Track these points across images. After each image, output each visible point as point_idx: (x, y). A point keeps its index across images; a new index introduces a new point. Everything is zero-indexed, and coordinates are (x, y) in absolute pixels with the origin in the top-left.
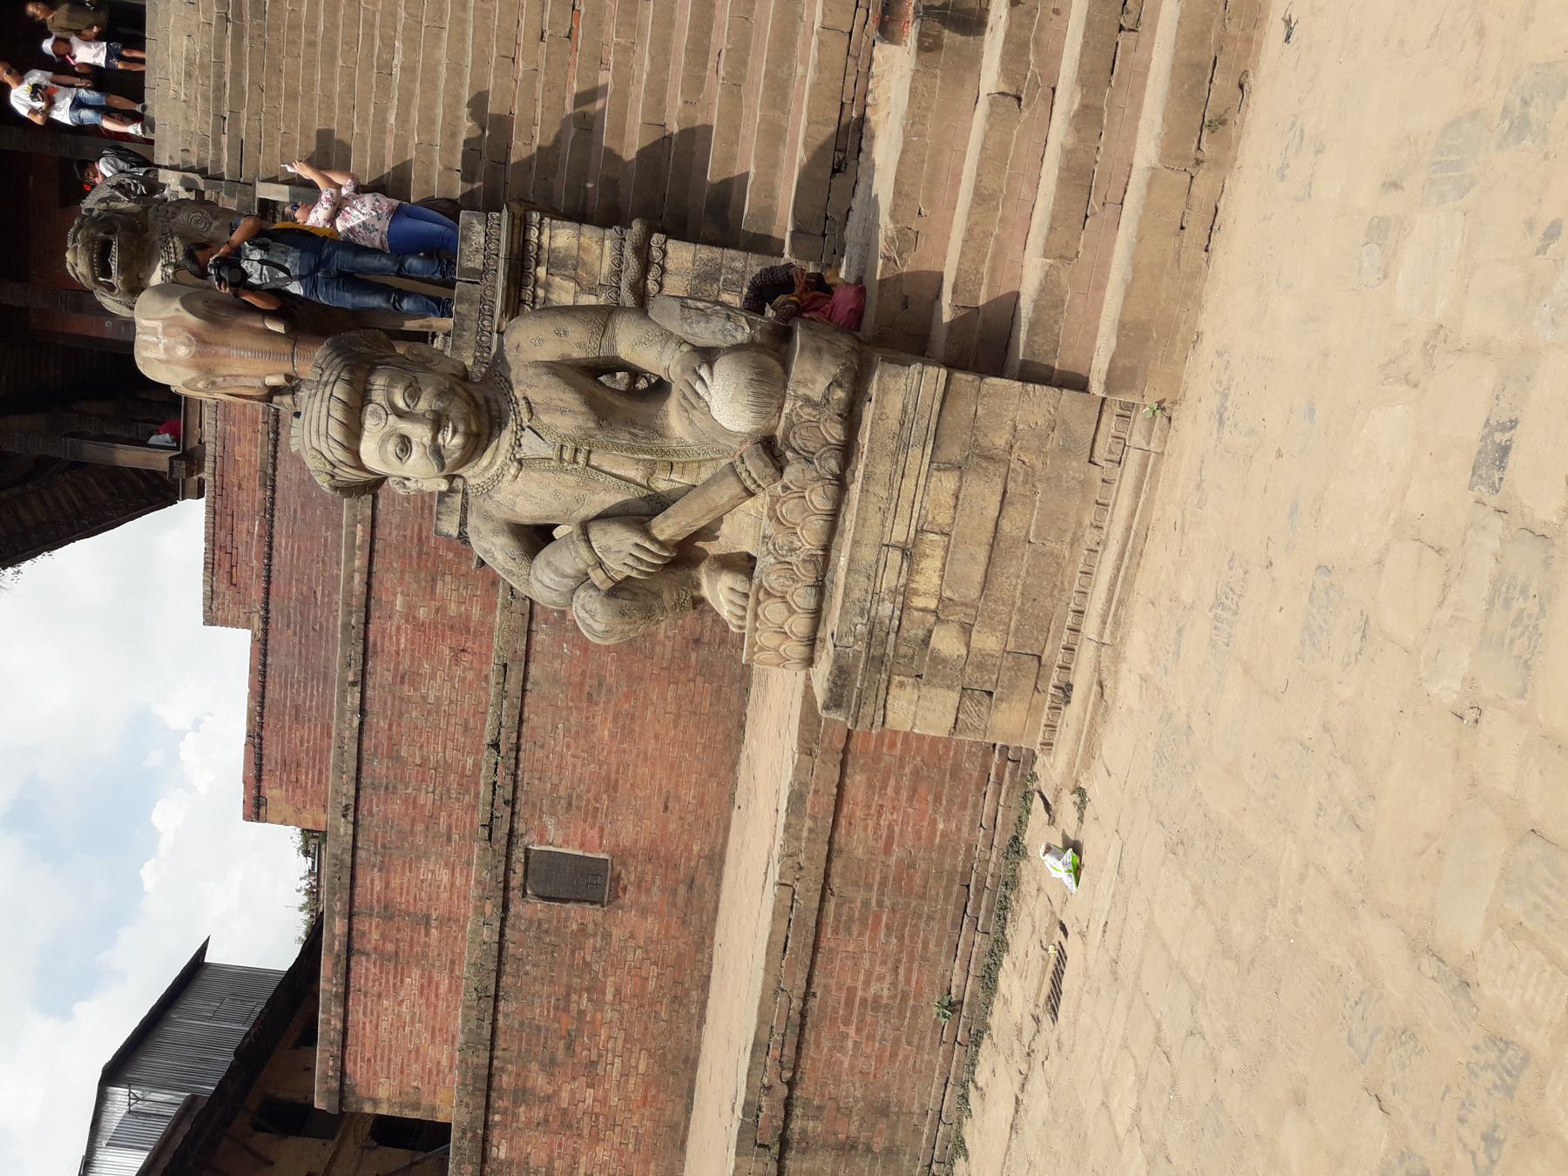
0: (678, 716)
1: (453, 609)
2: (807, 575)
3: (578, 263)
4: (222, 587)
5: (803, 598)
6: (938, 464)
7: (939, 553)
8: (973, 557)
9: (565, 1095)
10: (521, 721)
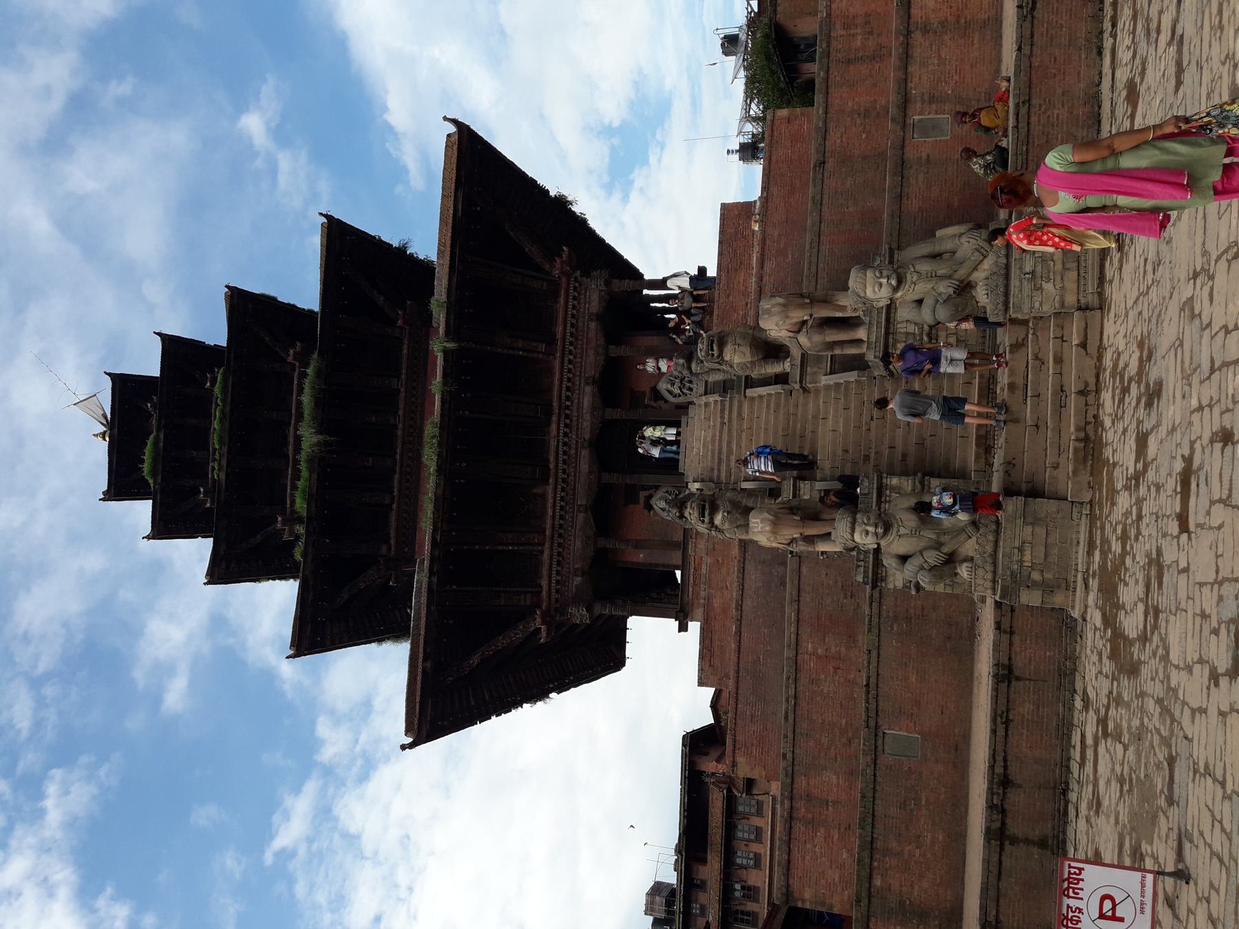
1: (833, 649)
2: (989, 560)
3: (900, 488)
4: (707, 668)
5: (989, 568)
9: (906, 852)
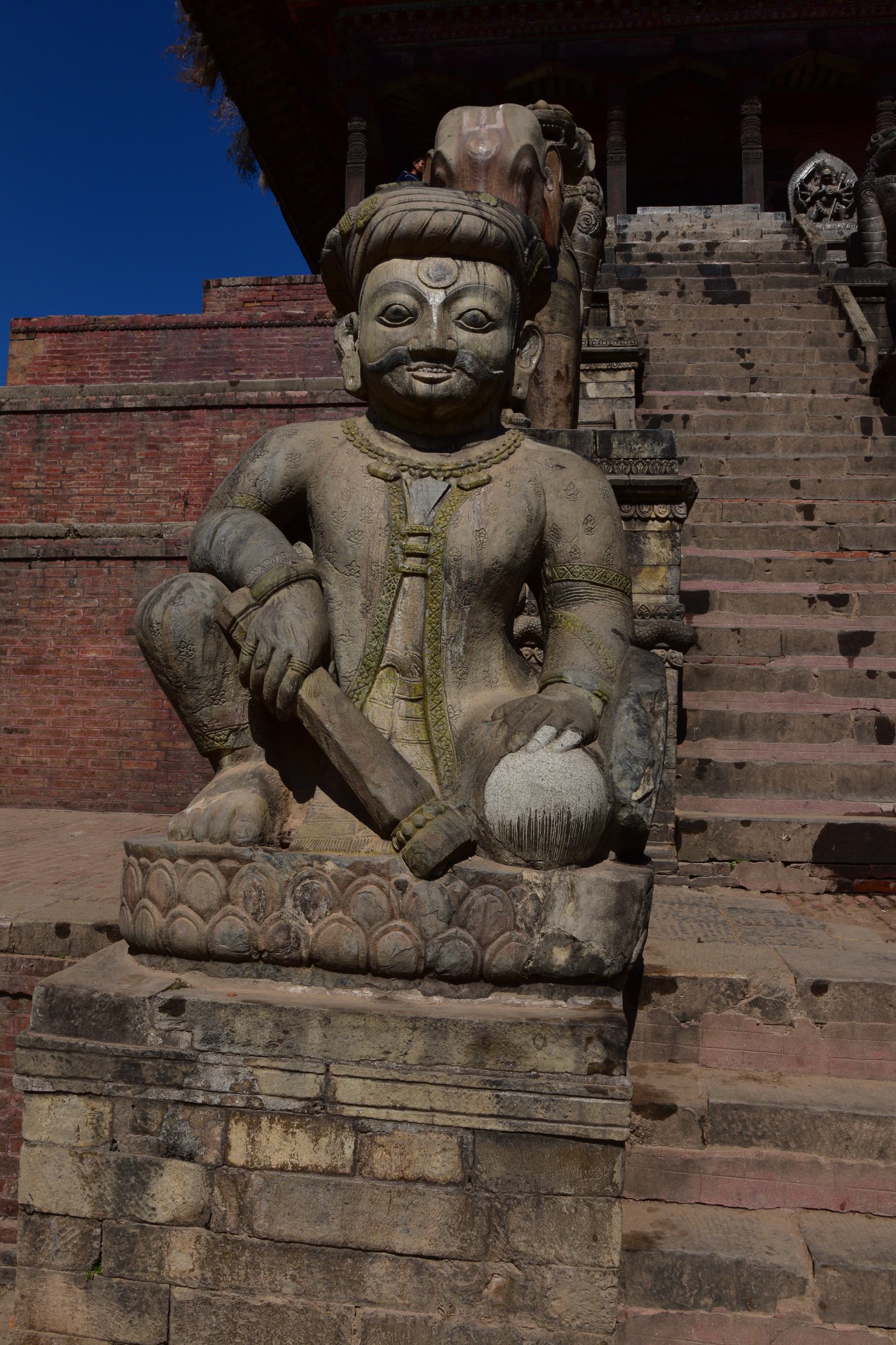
0: (116, 734)
4: (241, 295)
6: (472, 1144)
7: (323, 1160)
8: (323, 1218)
10: (98, 559)
